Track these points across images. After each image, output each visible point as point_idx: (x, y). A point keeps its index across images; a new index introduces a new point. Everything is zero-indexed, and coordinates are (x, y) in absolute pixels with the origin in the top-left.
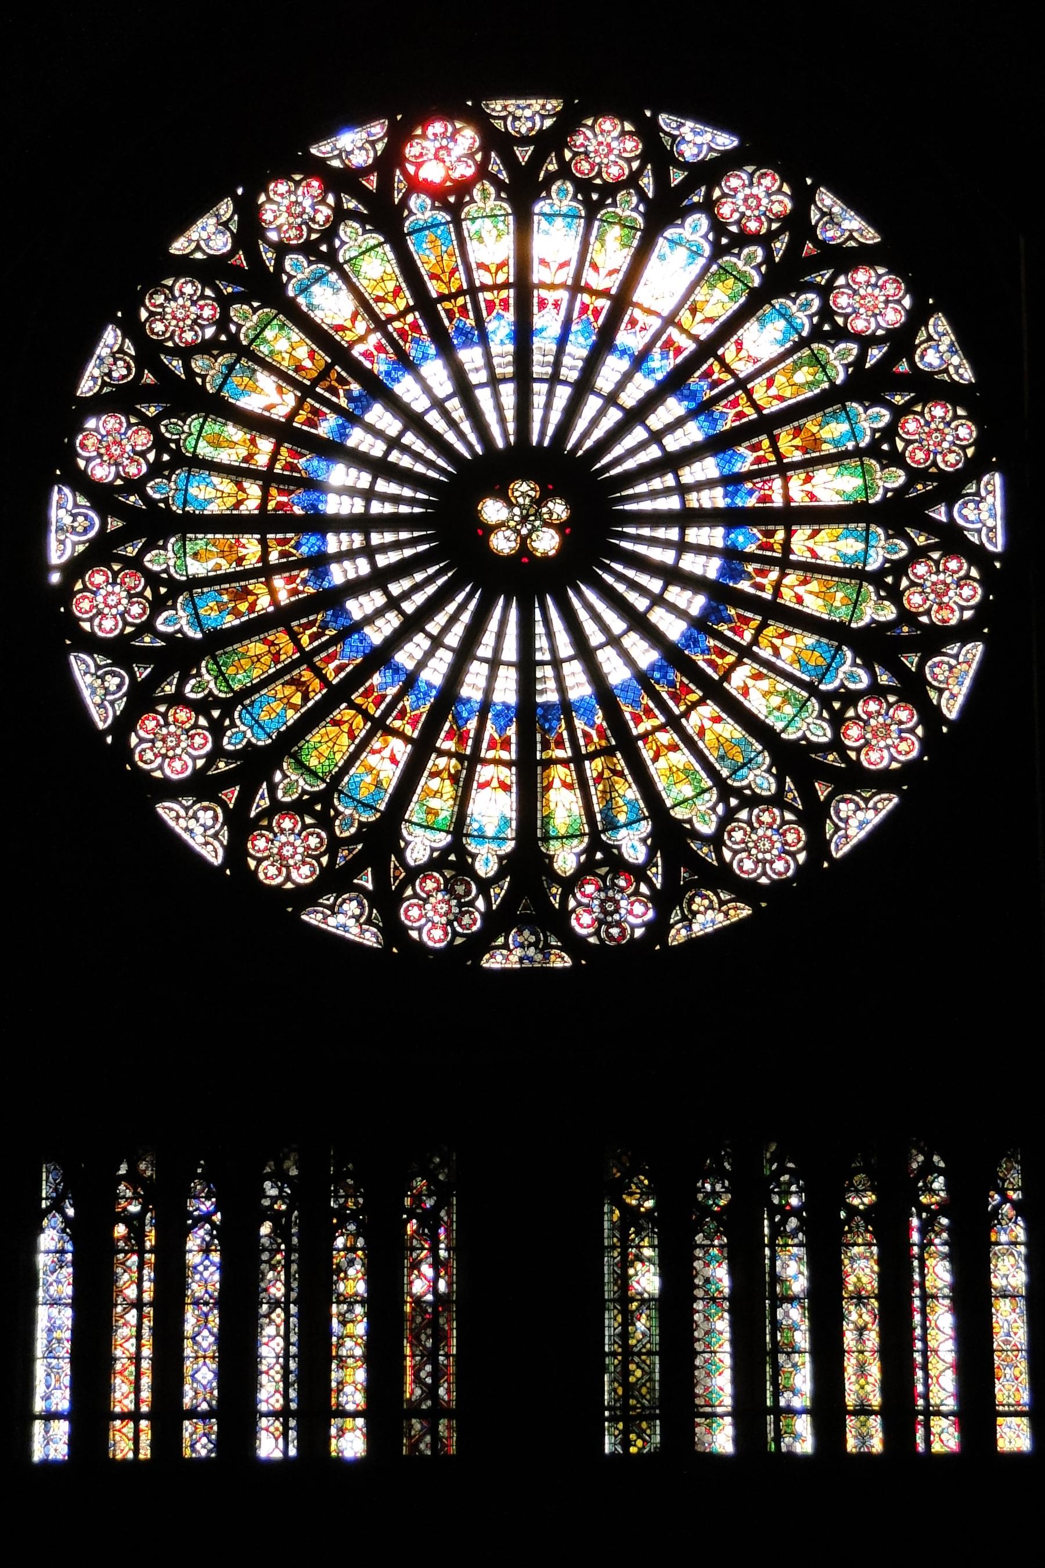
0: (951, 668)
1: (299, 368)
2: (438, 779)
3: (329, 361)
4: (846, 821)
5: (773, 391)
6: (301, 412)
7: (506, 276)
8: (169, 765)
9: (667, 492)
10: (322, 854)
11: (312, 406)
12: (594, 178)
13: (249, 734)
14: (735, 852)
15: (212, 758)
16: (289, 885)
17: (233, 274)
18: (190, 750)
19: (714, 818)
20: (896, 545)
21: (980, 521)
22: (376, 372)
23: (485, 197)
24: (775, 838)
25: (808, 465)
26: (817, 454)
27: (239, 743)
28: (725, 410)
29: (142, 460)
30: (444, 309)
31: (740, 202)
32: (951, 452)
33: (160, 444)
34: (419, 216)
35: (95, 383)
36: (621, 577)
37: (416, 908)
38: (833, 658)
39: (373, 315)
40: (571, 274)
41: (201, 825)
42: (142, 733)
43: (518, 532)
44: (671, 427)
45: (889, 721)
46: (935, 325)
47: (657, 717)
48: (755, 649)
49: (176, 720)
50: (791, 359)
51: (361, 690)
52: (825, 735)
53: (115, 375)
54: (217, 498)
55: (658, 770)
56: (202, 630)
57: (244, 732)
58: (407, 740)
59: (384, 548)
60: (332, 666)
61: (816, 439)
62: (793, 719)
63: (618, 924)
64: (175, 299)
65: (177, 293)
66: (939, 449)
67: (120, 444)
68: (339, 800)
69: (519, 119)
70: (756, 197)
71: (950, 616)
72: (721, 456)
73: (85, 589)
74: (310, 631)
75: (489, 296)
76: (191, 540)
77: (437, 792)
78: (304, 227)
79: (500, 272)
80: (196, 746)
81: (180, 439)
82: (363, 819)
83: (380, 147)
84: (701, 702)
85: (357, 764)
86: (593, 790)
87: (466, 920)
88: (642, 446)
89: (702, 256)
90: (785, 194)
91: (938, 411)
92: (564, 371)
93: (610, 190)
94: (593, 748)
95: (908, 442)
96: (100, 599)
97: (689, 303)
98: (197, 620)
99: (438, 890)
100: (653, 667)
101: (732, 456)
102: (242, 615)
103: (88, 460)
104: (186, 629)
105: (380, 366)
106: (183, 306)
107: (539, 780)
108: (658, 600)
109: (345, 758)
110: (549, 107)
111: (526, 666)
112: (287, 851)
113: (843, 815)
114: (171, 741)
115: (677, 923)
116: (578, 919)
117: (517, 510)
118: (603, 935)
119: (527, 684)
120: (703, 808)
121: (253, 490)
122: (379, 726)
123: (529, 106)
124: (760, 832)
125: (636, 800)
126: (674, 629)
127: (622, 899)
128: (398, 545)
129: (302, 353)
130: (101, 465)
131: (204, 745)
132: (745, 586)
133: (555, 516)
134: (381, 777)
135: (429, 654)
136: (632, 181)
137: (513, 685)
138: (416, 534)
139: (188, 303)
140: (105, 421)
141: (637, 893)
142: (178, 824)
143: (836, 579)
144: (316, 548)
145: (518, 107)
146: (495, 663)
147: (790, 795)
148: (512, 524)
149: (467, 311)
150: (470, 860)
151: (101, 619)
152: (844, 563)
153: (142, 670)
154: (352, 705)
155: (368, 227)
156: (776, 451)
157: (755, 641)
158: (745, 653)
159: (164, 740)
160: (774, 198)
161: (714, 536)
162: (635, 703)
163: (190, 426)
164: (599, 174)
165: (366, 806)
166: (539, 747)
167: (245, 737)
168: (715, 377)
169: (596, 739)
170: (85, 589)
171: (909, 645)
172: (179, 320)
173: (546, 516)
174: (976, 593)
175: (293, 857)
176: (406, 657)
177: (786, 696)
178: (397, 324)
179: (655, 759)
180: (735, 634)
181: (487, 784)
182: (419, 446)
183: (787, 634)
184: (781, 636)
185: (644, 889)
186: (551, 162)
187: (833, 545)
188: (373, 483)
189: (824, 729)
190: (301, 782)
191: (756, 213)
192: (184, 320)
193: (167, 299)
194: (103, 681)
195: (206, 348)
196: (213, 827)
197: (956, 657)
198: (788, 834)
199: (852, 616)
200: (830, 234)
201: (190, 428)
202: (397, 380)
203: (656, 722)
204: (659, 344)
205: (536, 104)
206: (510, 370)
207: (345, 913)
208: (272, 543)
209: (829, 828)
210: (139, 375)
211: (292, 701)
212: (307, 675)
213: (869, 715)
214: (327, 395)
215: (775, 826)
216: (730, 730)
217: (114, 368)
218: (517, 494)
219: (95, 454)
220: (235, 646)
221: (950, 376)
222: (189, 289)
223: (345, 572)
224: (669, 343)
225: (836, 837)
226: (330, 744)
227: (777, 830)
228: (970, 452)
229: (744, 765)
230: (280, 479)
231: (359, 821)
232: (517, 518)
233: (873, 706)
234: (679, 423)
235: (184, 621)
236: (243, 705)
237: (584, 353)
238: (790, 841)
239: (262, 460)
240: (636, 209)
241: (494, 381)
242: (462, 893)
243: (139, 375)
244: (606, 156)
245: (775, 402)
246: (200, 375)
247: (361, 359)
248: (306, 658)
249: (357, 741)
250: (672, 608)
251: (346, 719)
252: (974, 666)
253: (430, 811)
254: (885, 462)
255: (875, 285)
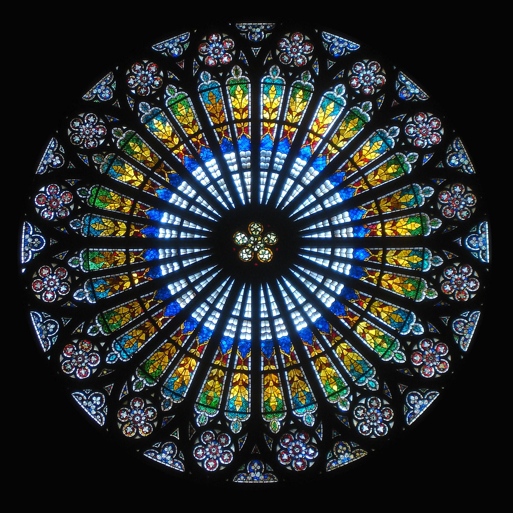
0: (465, 324)
1: (146, 162)
2: (212, 381)
3: (161, 158)
4: (413, 405)
5: (377, 177)
6: (146, 185)
7: (247, 115)
8: (78, 372)
9: (325, 229)
10: (154, 421)
11: (152, 181)
12: (291, 64)
13: (119, 356)
14: (359, 422)
15: (100, 368)
16: (138, 437)
17: (114, 112)
18: (89, 364)
19: (349, 403)
20: (438, 259)
21: (479, 247)
22: (184, 164)
23: (237, 74)
24: (379, 414)
25: (395, 216)
26: (399, 210)
27: (114, 360)
28: (354, 187)
29: (68, 210)
30: (217, 132)
31: (361, 78)
32: (465, 210)
33: (76, 201)
34: (205, 83)
35: (45, 168)
36: (303, 274)
37: (201, 450)
38: (407, 318)
39: (182, 135)
40: (279, 113)
41: (94, 404)
42: (65, 355)
43: (252, 249)
44: (327, 196)
45: (434, 353)
46: (456, 144)
47: (320, 349)
48: (369, 313)
49: (82, 348)
50: (386, 161)
51: (175, 332)
52: (403, 359)
53: (55, 163)
54: (104, 229)
55: (321, 377)
56: (96, 300)
57: (116, 355)
58: (197, 359)
59: (187, 257)
60: (160, 319)
61: (398, 203)
62: (387, 351)
63: (301, 460)
64: (85, 124)
65: (86, 121)
66: (459, 209)
67: (56, 200)
68: (164, 392)
69: (254, 33)
70: (369, 76)
71: (465, 297)
72: (352, 210)
73: (38, 277)
74: (150, 301)
75: (239, 125)
76: (91, 251)
77: (212, 387)
78: (148, 87)
79: (244, 113)
80: (92, 362)
81: (86, 198)
82: (175, 402)
83: (186, 46)
84: (342, 341)
85: (172, 372)
86: (289, 387)
87: (226, 457)
88: (313, 205)
89: (342, 106)
90: (383, 75)
91: (458, 189)
92: (275, 165)
93: (298, 70)
94: (289, 365)
95: (443, 205)
96: (46, 282)
97: (336, 130)
98: (93, 295)
99: (212, 440)
100: (318, 321)
101: (357, 211)
102: (116, 291)
103: (41, 208)
104: (88, 299)
105: (185, 160)
106: (89, 128)
107: (262, 382)
108: (321, 286)
109: (167, 369)
110: (268, 27)
111: (256, 320)
112: (137, 419)
113: (412, 402)
114: (80, 359)
115: (330, 459)
116: (281, 457)
117: (252, 238)
118: (294, 466)
119: (256, 331)
120: (343, 398)
121: (123, 226)
122: (184, 353)
123: (259, 27)
124: (371, 411)
125: (310, 392)
126: (329, 302)
127: (303, 446)
128: (193, 255)
129: (147, 153)
130: (47, 211)
131: (96, 361)
132: (363, 279)
133: (271, 242)
134: (185, 379)
135: (208, 314)
136: (308, 67)
137: (249, 331)
138: (202, 250)
139: (91, 127)
140: (49, 188)
141: (310, 443)
142: (82, 404)
143: (408, 276)
144: (153, 257)
145: (253, 27)
146: (241, 319)
147: (386, 391)
148: (250, 245)
149: (229, 133)
150: (228, 425)
151: (46, 293)
152: (412, 268)
153: (66, 321)
154: (170, 341)
155: (180, 88)
156: (379, 209)
157: (368, 309)
158: (364, 315)
159: (76, 359)
160: (377, 76)
161: (349, 253)
162: (309, 340)
163: (91, 191)
164: (293, 63)
165: (177, 395)
166: (262, 364)
167: (117, 357)
168: (349, 169)
169: (291, 360)
170: (38, 277)
171: (445, 311)
172: (86, 135)
173: (266, 242)
174: (477, 285)
175: (140, 422)
176: (197, 315)
177: (383, 337)
178: (194, 140)
179: (319, 372)
180: (359, 305)
181: (237, 383)
182: (204, 203)
183: (384, 305)
184: (381, 307)
185: (314, 441)
186: (269, 56)
187: (406, 258)
188: (182, 223)
189: (403, 356)
190: (145, 382)
191: (369, 84)
192: (89, 135)
193: (80, 124)
194: (47, 327)
195: (100, 150)
196: (100, 405)
197: (467, 318)
198: (385, 412)
199: (416, 296)
200: (405, 95)
201: (91, 193)
202: (194, 169)
203: (319, 352)
204: (322, 151)
205: (262, 25)
206: (249, 164)
207: (166, 453)
208: (131, 254)
209: (405, 411)
210: (67, 164)
211: (140, 338)
212: (148, 324)
213: (425, 349)
214: (160, 176)
215: (379, 408)
216: (356, 356)
217: (54, 160)
218: (252, 229)
219: (44, 205)
220: (112, 309)
221: (463, 170)
222: (91, 119)
223: (167, 269)
224: (327, 151)
225: (409, 414)
226: (159, 361)
227: (380, 410)
228: (474, 210)
229: (363, 375)
230: (136, 220)
231: (173, 403)
232: (252, 242)
233: (427, 345)
234: (331, 193)
235: (87, 295)
236: (116, 340)
237: (285, 156)
238: (386, 416)
239: (127, 209)
240: (310, 81)
241: (241, 170)
242: (224, 442)
243: (67, 164)
244: (296, 53)
245: (379, 183)
246: (96, 164)
247: (176, 157)
248: (148, 315)
249: (173, 360)
250: (328, 291)
251: (167, 348)
252: (476, 324)
253: (208, 398)
254: (432, 215)
255: (427, 123)
